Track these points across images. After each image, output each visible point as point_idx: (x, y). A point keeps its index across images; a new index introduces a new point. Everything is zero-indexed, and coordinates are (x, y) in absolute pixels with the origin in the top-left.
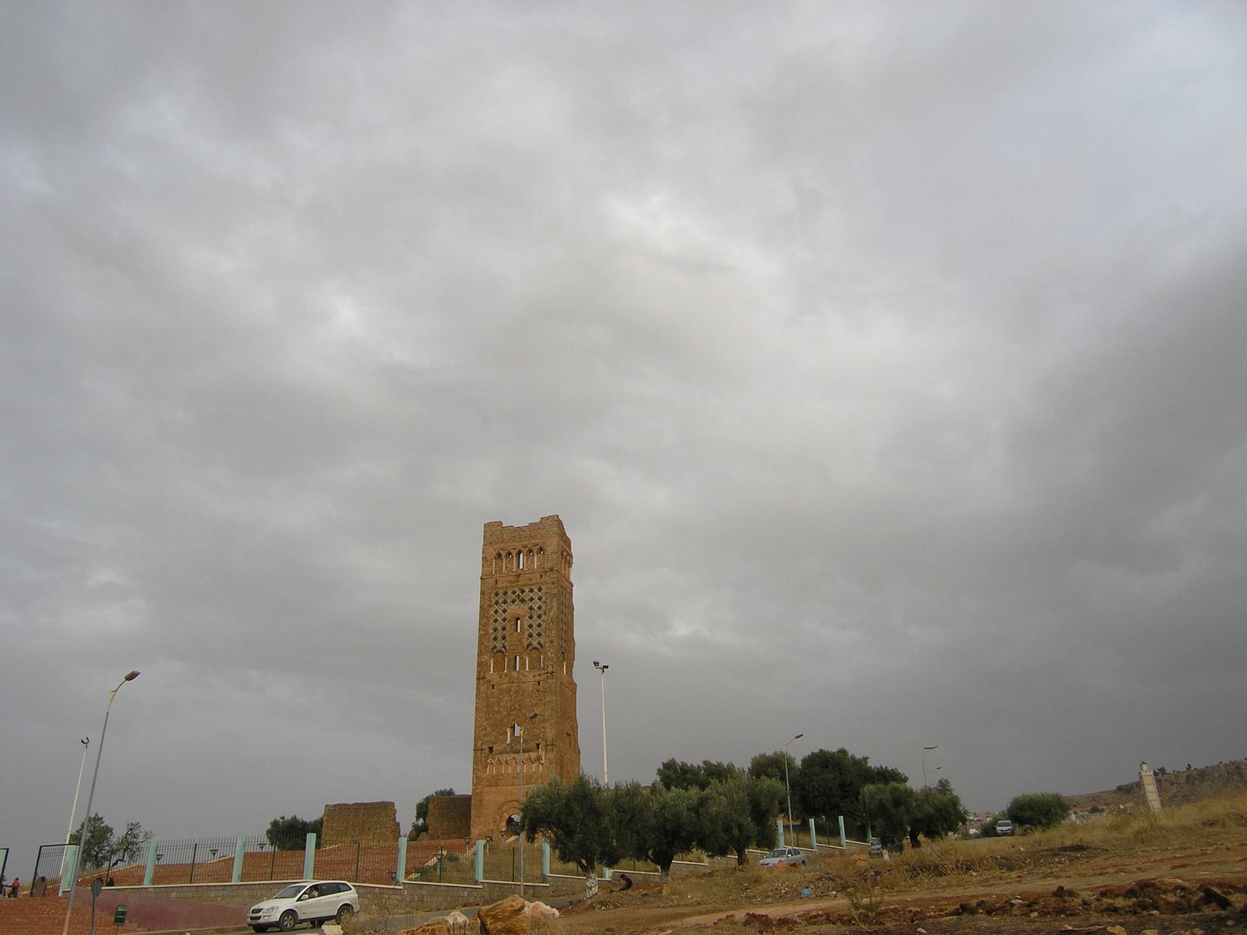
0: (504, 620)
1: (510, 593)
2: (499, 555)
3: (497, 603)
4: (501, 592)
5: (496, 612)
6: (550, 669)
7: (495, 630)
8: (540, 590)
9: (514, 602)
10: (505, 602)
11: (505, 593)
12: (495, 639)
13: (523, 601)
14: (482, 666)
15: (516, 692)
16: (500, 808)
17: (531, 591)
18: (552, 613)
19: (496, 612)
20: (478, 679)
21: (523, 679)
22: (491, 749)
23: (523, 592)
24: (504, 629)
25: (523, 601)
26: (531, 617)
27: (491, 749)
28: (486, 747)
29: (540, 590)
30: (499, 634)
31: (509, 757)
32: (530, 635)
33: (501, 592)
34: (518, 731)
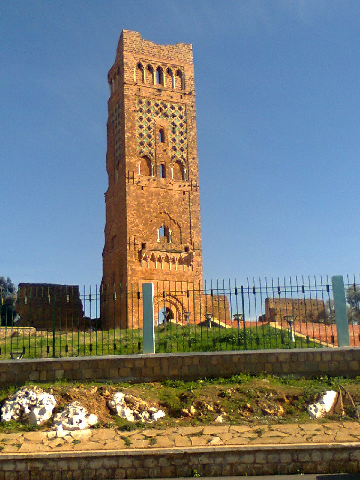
1: (153, 104)
2: (140, 66)
3: (141, 110)
6: (194, 183)
7: (141, 135)
9: (157, 113)
10: (149, 111)
11: (149, 104)
12: (142, 144)
13: (166, 115)
15: (164, 197)
17: (173, 108)
18: (192, 133)
19: (141, 118)
21: (171, 187)
22: (143, 246)
23: (165, 107)
25: (166, 115)
26: (174, 132)
27: (143, 246)
28: (139, 242)
29: (180, 109)
32: (175, 149)
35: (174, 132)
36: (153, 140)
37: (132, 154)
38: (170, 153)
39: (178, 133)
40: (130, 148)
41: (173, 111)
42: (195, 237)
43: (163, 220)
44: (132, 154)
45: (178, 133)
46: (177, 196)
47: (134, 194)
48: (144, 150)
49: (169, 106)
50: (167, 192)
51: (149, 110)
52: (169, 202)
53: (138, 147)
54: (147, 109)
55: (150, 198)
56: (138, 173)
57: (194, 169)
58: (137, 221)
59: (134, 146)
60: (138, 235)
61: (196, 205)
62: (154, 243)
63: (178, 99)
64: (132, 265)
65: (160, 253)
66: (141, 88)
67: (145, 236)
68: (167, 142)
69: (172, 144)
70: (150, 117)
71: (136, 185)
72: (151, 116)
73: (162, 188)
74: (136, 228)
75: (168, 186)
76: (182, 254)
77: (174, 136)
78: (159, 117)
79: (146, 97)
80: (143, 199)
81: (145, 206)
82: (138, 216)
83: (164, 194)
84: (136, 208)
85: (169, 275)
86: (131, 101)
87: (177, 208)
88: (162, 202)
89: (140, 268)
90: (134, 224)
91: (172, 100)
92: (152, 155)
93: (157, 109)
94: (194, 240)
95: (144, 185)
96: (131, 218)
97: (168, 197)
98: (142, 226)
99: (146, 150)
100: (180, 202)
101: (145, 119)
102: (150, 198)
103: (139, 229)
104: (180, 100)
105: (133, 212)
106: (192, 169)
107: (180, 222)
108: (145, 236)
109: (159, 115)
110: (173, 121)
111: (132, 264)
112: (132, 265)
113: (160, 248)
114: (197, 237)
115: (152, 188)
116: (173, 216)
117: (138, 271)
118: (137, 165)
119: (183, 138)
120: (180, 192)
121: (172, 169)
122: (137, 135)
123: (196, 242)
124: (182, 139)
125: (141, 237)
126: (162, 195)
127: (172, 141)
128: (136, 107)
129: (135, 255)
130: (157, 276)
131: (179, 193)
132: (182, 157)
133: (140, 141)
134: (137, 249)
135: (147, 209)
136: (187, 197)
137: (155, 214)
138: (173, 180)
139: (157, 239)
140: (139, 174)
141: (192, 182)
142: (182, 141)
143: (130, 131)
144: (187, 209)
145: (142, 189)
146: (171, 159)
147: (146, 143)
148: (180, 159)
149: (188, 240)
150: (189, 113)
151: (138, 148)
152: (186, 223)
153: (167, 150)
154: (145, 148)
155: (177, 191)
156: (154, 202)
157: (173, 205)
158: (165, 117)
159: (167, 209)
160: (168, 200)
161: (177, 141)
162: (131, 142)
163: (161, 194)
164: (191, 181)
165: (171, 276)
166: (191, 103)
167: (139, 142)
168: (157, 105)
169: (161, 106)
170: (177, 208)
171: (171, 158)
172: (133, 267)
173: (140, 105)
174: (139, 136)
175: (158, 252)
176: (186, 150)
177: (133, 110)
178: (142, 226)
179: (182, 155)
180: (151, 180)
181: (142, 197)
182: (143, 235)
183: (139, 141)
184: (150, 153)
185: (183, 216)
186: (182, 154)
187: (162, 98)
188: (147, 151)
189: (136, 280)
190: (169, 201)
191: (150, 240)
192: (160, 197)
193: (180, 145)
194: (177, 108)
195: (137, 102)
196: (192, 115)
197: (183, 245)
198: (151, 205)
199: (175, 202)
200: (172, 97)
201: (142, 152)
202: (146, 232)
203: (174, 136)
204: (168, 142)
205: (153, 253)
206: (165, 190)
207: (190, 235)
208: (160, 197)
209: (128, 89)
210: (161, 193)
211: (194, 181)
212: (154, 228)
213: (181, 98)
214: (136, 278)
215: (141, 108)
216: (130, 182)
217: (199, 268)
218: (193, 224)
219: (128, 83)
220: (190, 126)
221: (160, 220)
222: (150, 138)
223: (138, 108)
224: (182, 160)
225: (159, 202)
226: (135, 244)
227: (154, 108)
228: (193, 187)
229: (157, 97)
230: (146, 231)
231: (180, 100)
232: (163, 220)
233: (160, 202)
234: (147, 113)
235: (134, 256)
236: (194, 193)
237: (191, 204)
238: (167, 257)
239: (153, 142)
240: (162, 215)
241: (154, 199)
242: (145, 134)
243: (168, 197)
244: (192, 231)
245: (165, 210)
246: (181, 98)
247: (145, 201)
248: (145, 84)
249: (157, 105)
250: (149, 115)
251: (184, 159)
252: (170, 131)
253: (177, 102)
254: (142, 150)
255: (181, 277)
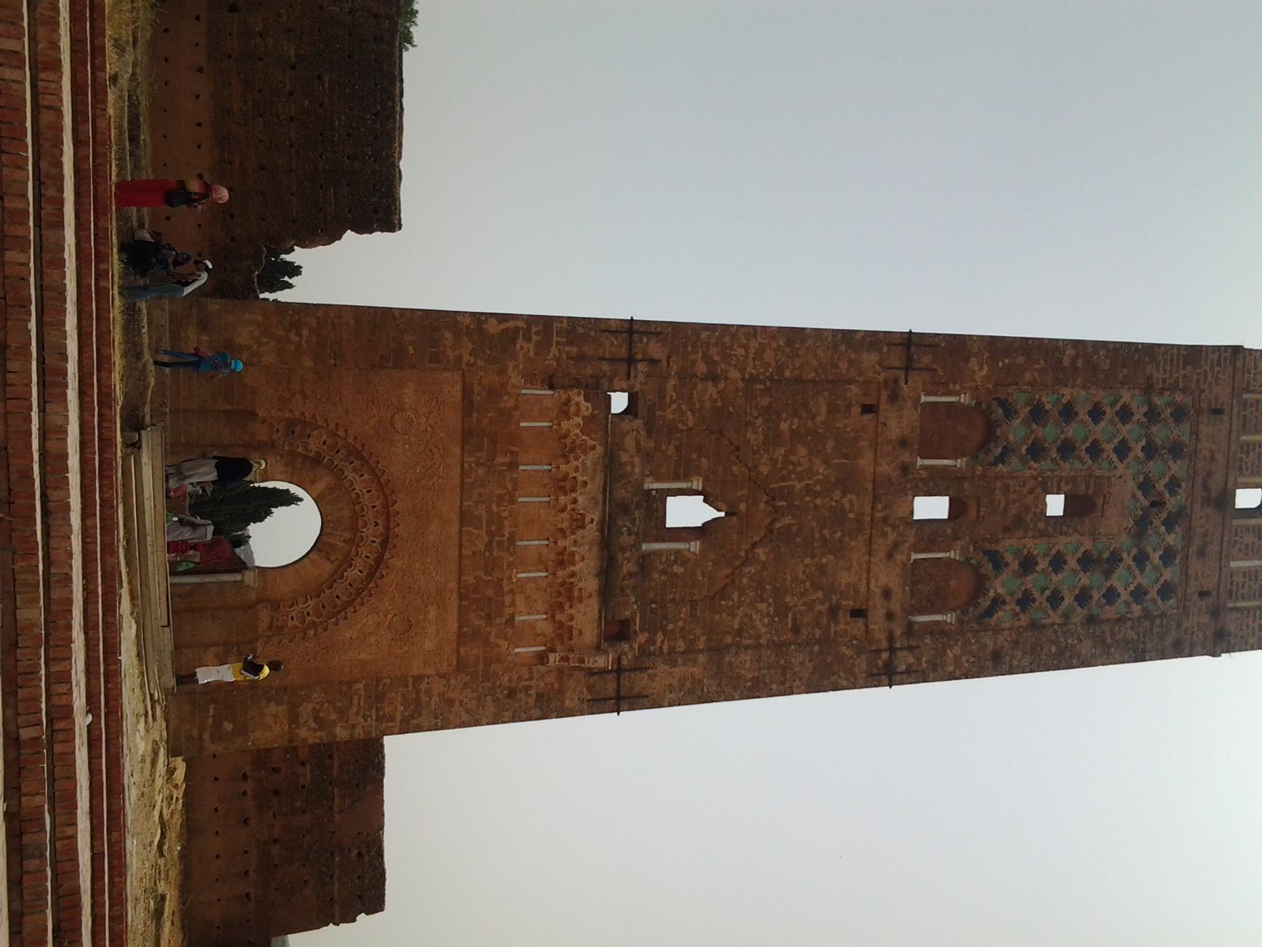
0: (1095, 450)
1: (1178, 468)
3: (1153, 415)
4: (1182, 432)
5: (1125, 414)
7: (1068, 412)
8: (1166, 591)
9: (1146, 486)
10: (1151, 451)
11: (1176, 450)
12: (1038, 413)
13: (1142, 524)
14: (954, 349)
16: (357, 455)
19: (1125, 414)
20: (910, 341)
21: (881, 545)
23: (1169, 524)
24: (1067, 449)
25: (1142, 524)
26: (1087, 562)
29: (1166, 591)
30: (1049, 432)
31: (586, 500)
32: (1028, 564)
33: (1182, 432)
34: (688, 511)
35: (1087, 562)
36: (1052, 466)
37: (1000, 364)
38: (1008, 546)
39: (1085, 579)
40: (1021, 360)
41: (1155, 557)
42: (678, 671)
43: (743, 506)
44: (1000, 364)
45: (1085, 579)
46: (845, 578)
47: (843, 365)
48: (1017, 422)
49: (1171, 539)
50: (860, 530)
51: (1157, 450)
52: (817, 536)
53: (1022, 398)
54: (1159, 442)
55: (830, 444)
56: (928, 394)
57: (957, 659)
58: (734, 374)
59: (1028, 376)
60: (672, 382)
61: (813, 673)
62: (637, 460)
63: (1196, 579)
64: (529, 341)
65: (594, 487)
66: (1226, 418)
67: (669, 414)
68: (1050, 530)
69: (1045, 555)
70: (1131, 455)
71: (881, 378)
72: (1137, 458)
73: (876, 499)
74: (702, 368)
75: (884, 534)
76: (593, 605)
77: (1072, 563)
78: (1134, 496)
79: (1198, 440)
80: (824, 409)
81: (796, 421)
82: (754, 379)
83: (851, 515)
84: (788, 374)
85: (489, 533)
86: (1182, 372)
87: (795, 580)
88: (819, 501)
89: (515, 379)
90: (716, 358)
91: (1193, 549)
92: (995, 463)
93: (1160, 486)
94: (663, 667)
95: (881, 419)
96: (746, 347)
97: (839, 534)
98: (714, 401)
99: (1016, 431)
100: (820, 594)
101: (1125, 430)
102: (830, 444)
103: (700, 387)
104: (1193, 588)
105: (769, 355)
106: (957, 650)
107: (735, 596)
108: (669, 414)
109: (1139, 494)
110: (1125, 555)
111: (534, 338)
112: (529, 341)
113: (621, 493)
114: (674, 682)
115: (871, 456)
116: (763, 557)
117: (503, 371)
118: (957, 387)
119: (1066, 602)
120: (863, 589)
121: (952, 554)
122: (1067, 393)
123: (652, 678)
124: (1063, 599)
125: (661, 391)
126: (845, 502)
127: (1053, 552)
128: (1161, 393)
129: (581, 358)
130: (481, 471)
131: (856, 591)
132: (997, 602)
133: (1048, 407)
134: (605, 367)
135: (784, 426)
136: (842, 626)
137: (764, 469)
138: (909, 556)
139: (659, 479)
140: (924, 399)
141: (905, 653)
142: (1055, 599)
143: (1080, 364)
144: (796, 630)
145: (867, 409)
146: (988, 546)
147: (1041, 432)
148: (992, 594)
149: (660, 637)
150: (1156, 630)
151: (1019, 398)
152: (736, 627)
153: (1019, 534)
154: (1022, 431)
155: (865, 576)
156: (817, 461)
157: (808, 561)
158: (1137, 523)
159: (789, 527)
160: (826, 532)
161: (1056, 578)
162: (1042, 361)
163: (849, 496)
164: (910, 648)
165: (488, 546)
166: (1188, 637)
167: (1044, 399)
168: (1173, 485)
169: (1172, 503)
170: (795, 580)
171: (993, 547)
172: (520, 342)
173: (1169, 411)
174: (1064, 401)
175: (599, 479)
176: (1024, 620)
177: (1150, 377)
178: (714, 401)
179: (1004, 602)
180: (905, 456)
181: (832, 408)
182: (672, 401)
183: (1048, 400)
184: (1006, 451)
185: (763, 606)
186: (1008, 599)
187: (1197, 507)
188: (1011, 438)
189: (459, 359)
190: (823, 538)
191: (652, 444)
192: (837, 494)
193: (1043, 590)
194: (1167, 575)
195: (1179, 397)
196: (1149, 645)
197: (634, 614)
198: (802, 451)
199: (822, 569)
200: (1201, 553)
201: (1010, 412)
202: (685, 423)
203: (1072, 563)
204: (1050, 536)
205: (593, 448)
206: (867, 519)
207: (681, 645)
208: (837, 494)
209: (1219, 364)
210: (853, 497)
211: (912, 660)
212: (704, 461)
213: (1203, 594)
214: (467, 358)
215: (1159, 415)
216: (893, 348)
217: (532, 701)
218: (731, 663)
219: (1239, 364)
220: (1113, 634)
221: (739, 493)
222: (1059, 450)
223: (1159, 401)
224: (985, 603)
225: (818, 488)
226: (631, 360)
227: (1164, 475)
228: (885, 655)
229: (1198, 486)
230: (691, 424)
231: (1193, 588)
232: (743, 506)
233: (816, 495)
234: (1143, 443)
235: (574, 350)
236: (862, 663)
237: (816, 648)
238: (579, 523)
239: (1046, 464)
240: (762, 506)
241: (826, 461)
242: (1073, 430)
243: (839, 534)
244: (702, 659)
245: (788, 520)
246: (1203, 594)
247: (819, 419)
248: (1238, 438)
249: (1173, 485)
250: (1137, 450)
251: (990, 612)
252: (1088, 544)
253: (1187, 574)
254: (1016, 412)
255: (482, 602)
